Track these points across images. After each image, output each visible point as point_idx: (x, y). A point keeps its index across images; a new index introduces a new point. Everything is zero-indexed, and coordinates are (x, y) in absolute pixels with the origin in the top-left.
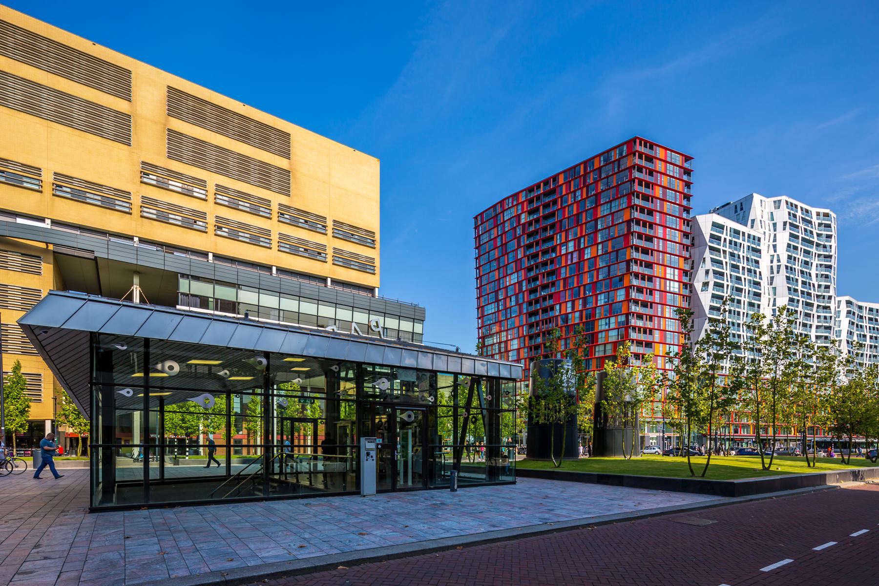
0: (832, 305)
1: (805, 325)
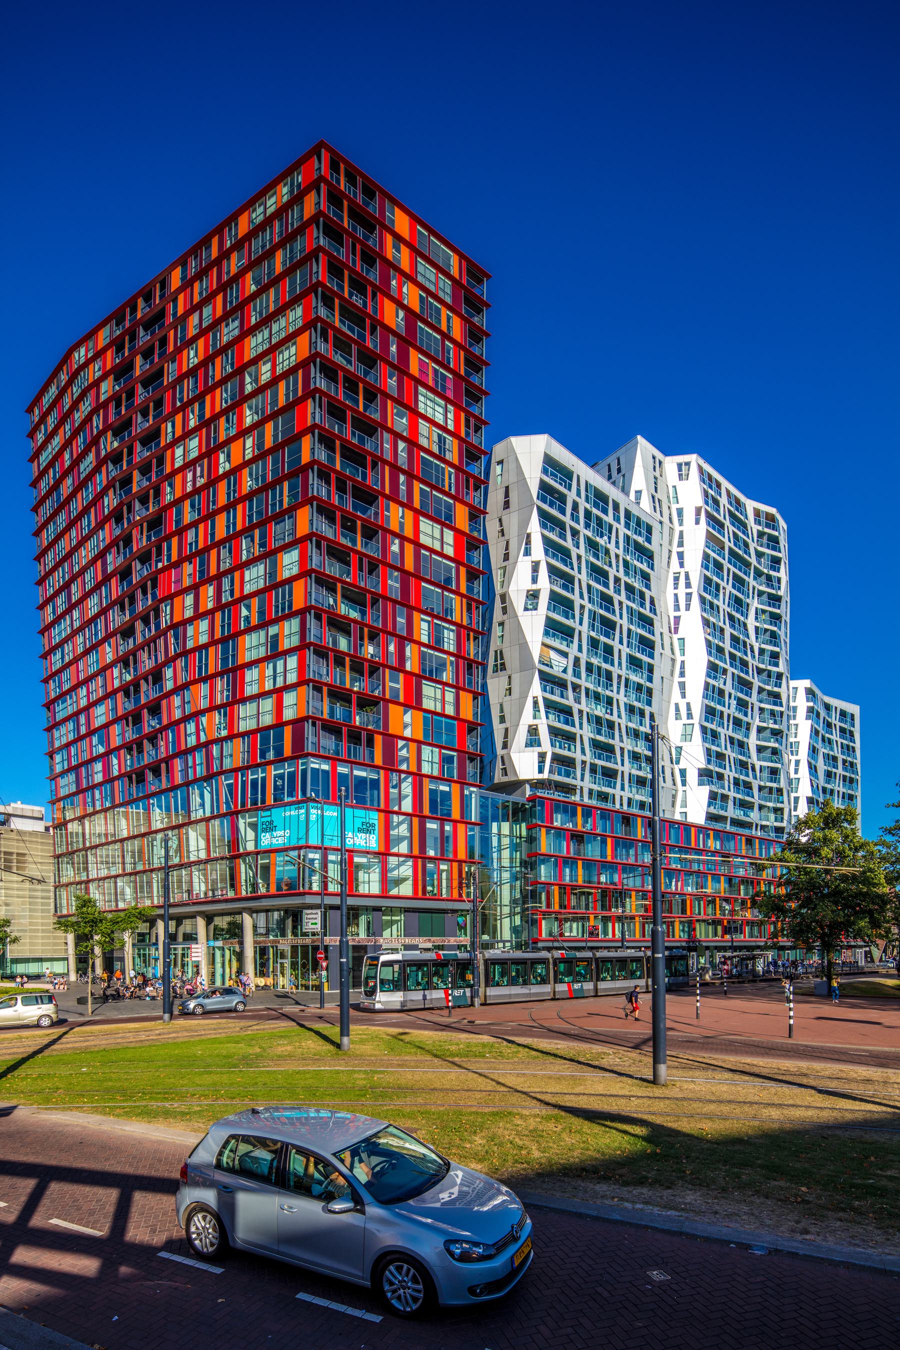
0: (783, 691)
1: (737, 723)
